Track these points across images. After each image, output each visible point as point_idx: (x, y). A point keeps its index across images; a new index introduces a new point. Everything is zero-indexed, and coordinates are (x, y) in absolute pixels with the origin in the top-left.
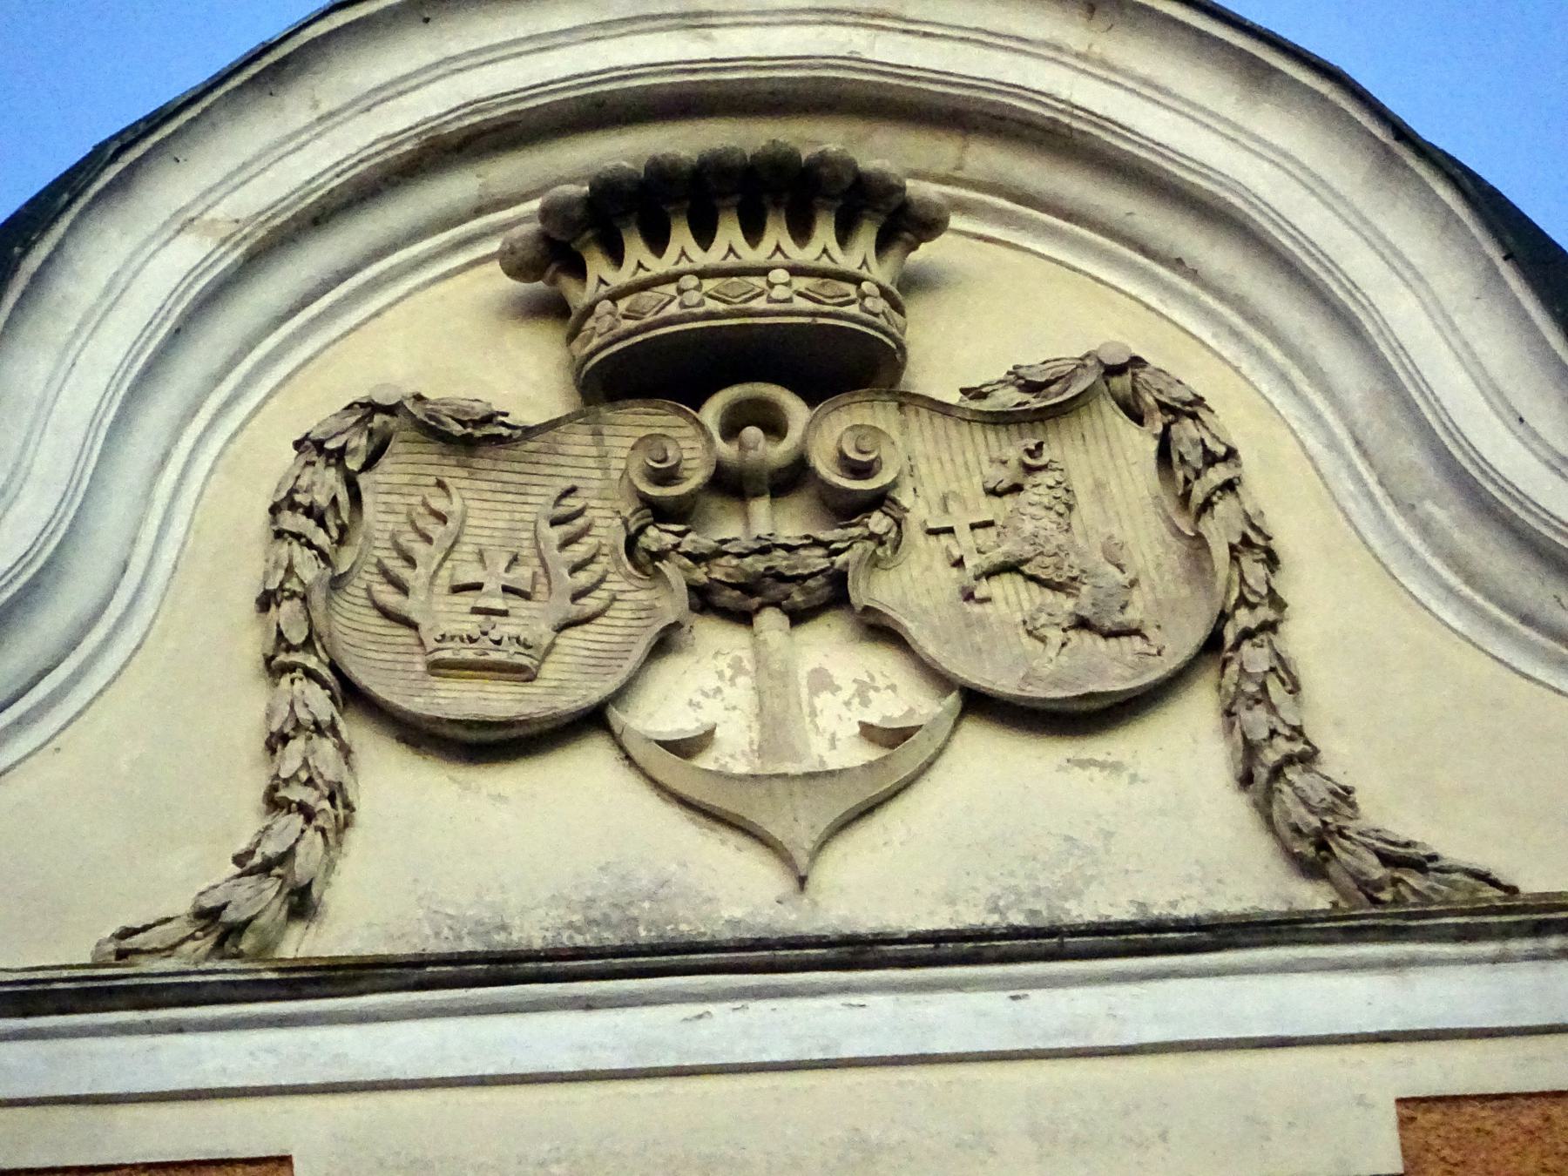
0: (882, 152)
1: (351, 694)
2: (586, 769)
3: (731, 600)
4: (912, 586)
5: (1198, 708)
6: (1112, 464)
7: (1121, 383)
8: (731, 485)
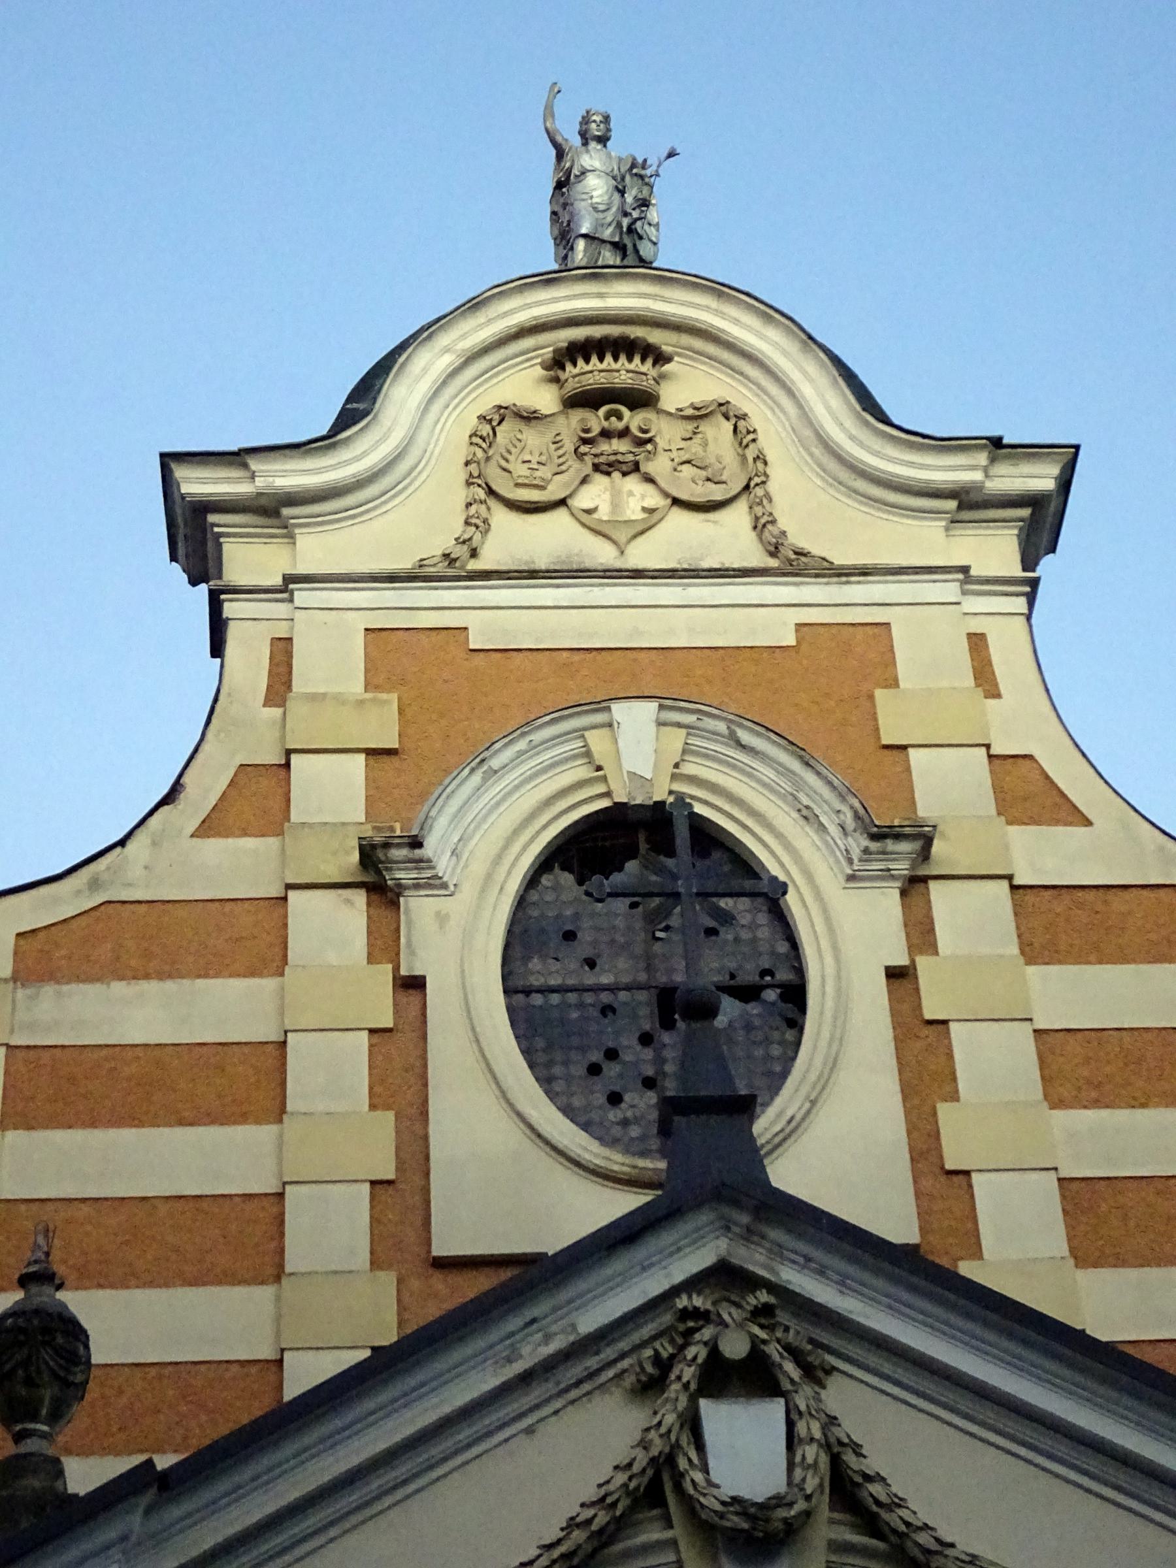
0: (655, 337)
1: (491, 492)
2: (561, 514)
3: (604, 468)
4: (658, 466)
5: (741, 506)
6: (719, 432)
7: (723, 409)
8: (606, 434)
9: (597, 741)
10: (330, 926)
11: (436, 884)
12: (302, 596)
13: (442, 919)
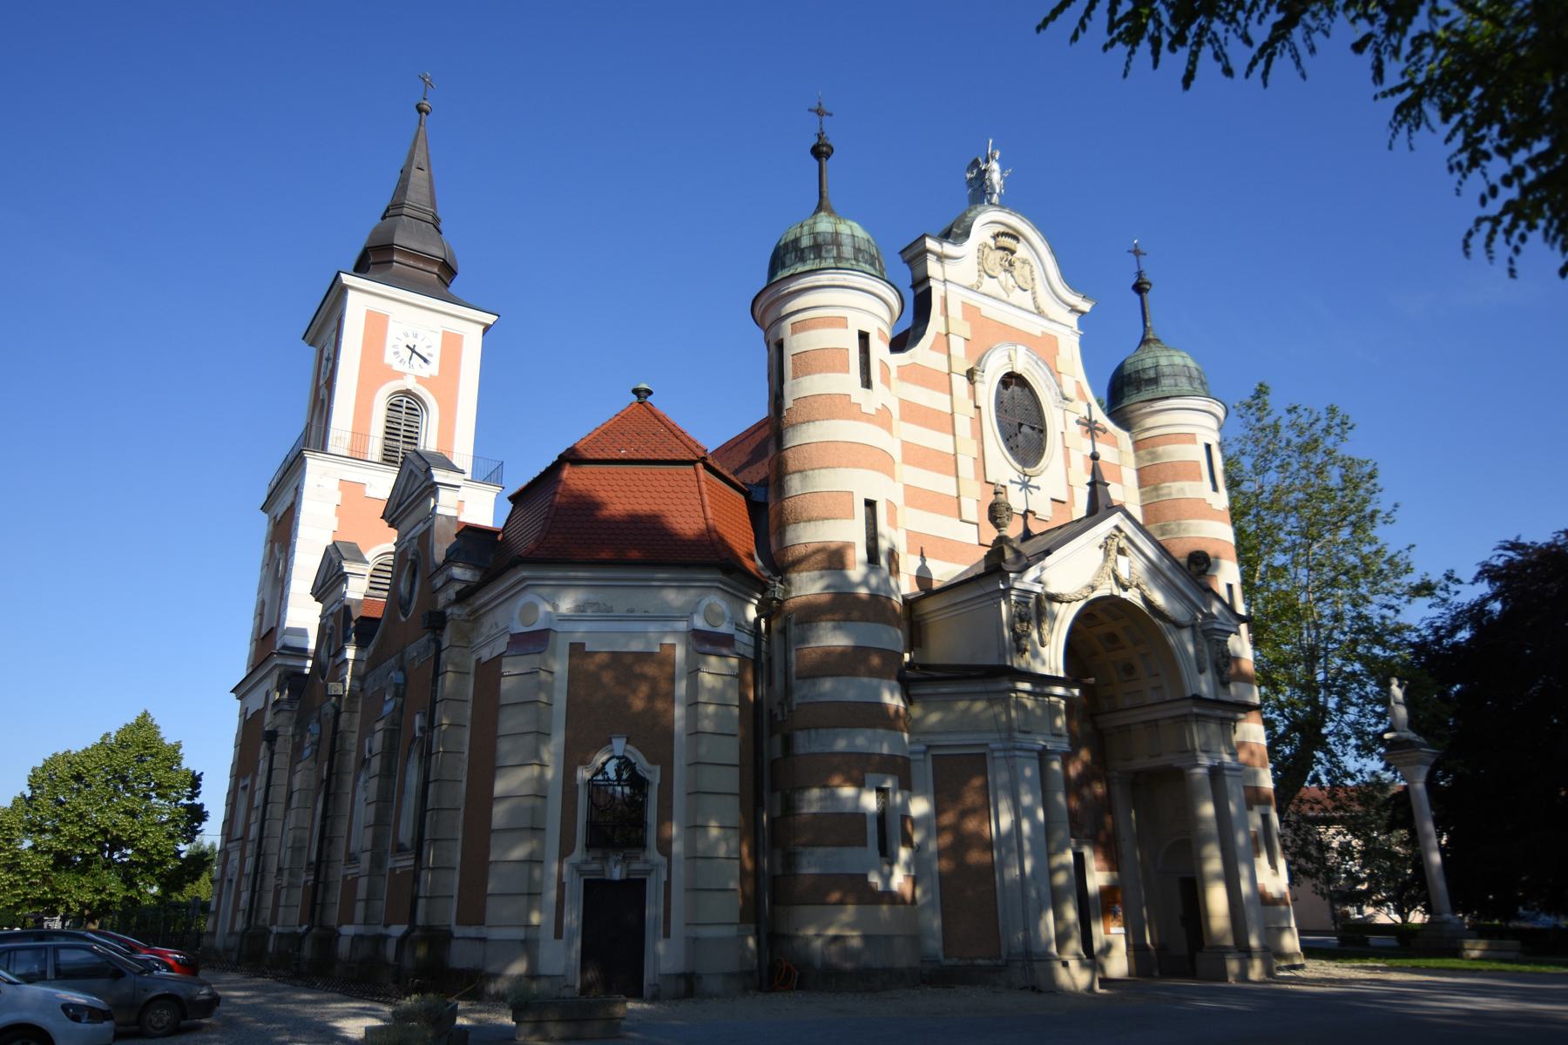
6: (1027, 268)
10: (960, 383)
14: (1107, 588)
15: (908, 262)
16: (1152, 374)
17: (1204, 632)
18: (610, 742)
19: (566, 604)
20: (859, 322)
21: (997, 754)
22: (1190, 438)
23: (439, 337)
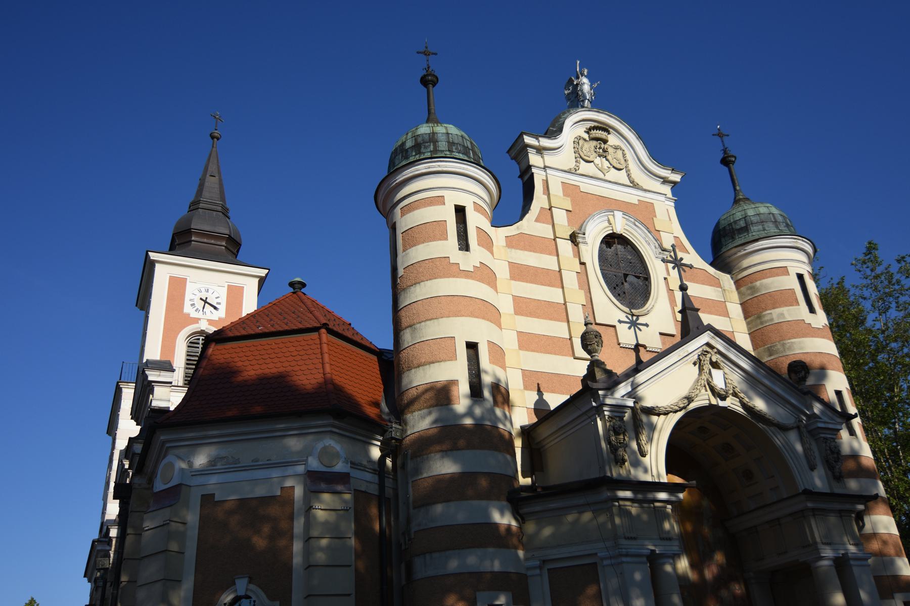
1: (581, 157)
3: (600, 156)
4: (609, 157)
6: (620, 152)
9: (611, 218)
10: (565, 247)
11: (586, 243)
12: (548, 171)
13: (587, 251)
14: (704, 399)
15: (514, 158)
16: (742, 223)
17: (810, 432)
18: (234, 584)
19: (200, 460)
20: (453, 199)
21: (606, 562)
22: (784, 271)
23: (225, 290)
